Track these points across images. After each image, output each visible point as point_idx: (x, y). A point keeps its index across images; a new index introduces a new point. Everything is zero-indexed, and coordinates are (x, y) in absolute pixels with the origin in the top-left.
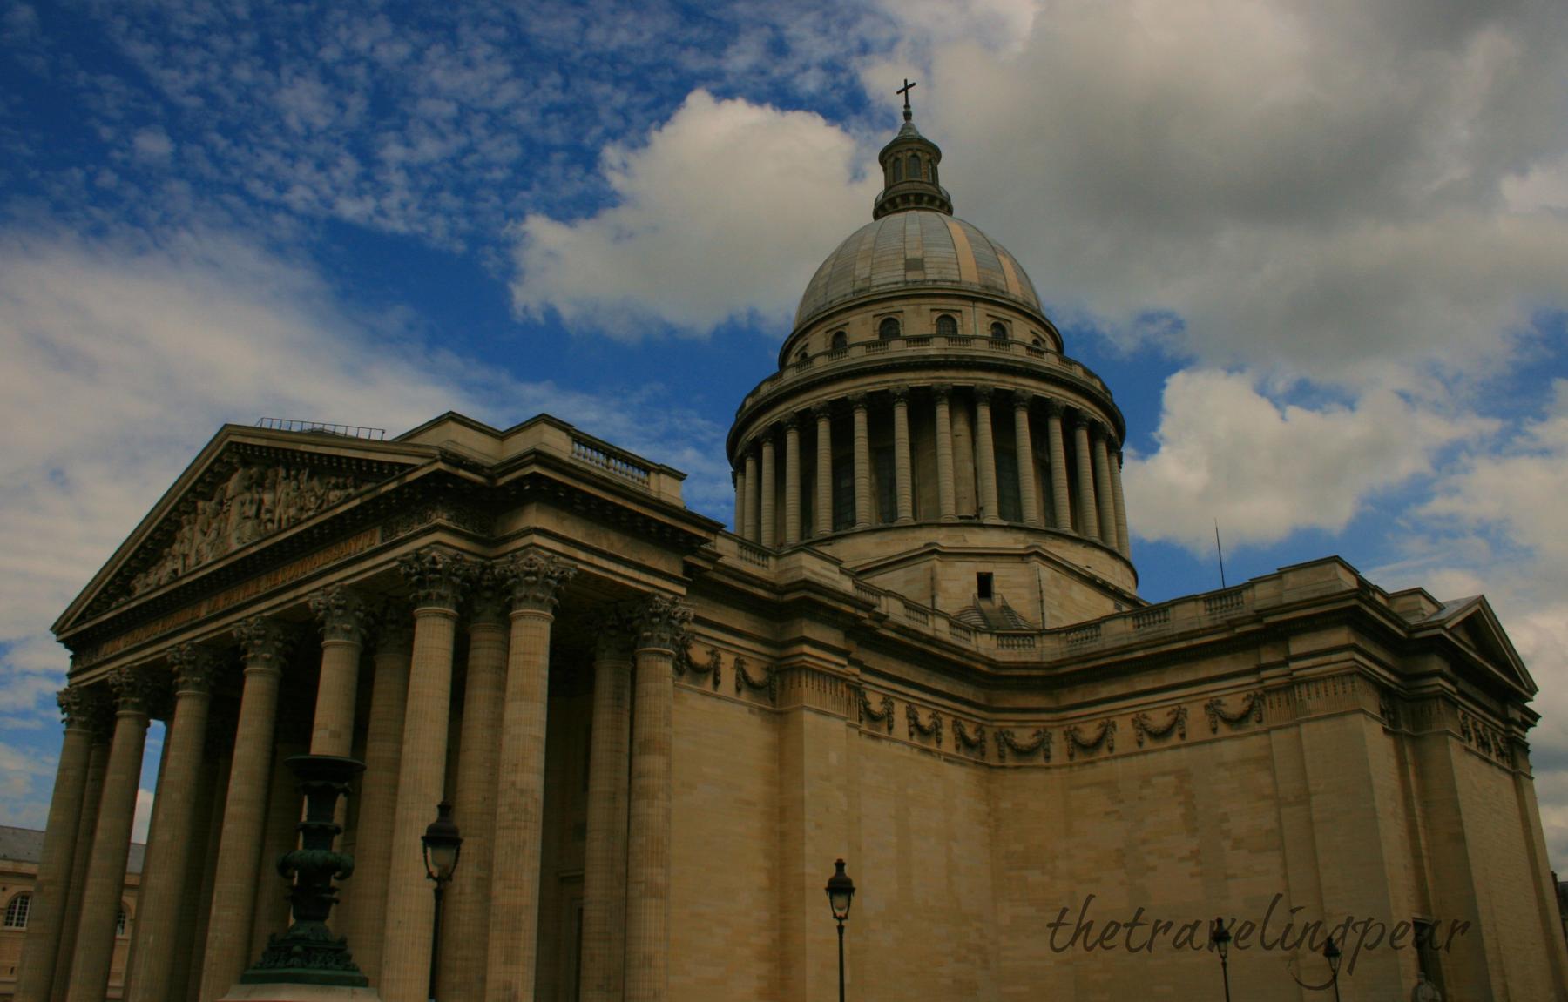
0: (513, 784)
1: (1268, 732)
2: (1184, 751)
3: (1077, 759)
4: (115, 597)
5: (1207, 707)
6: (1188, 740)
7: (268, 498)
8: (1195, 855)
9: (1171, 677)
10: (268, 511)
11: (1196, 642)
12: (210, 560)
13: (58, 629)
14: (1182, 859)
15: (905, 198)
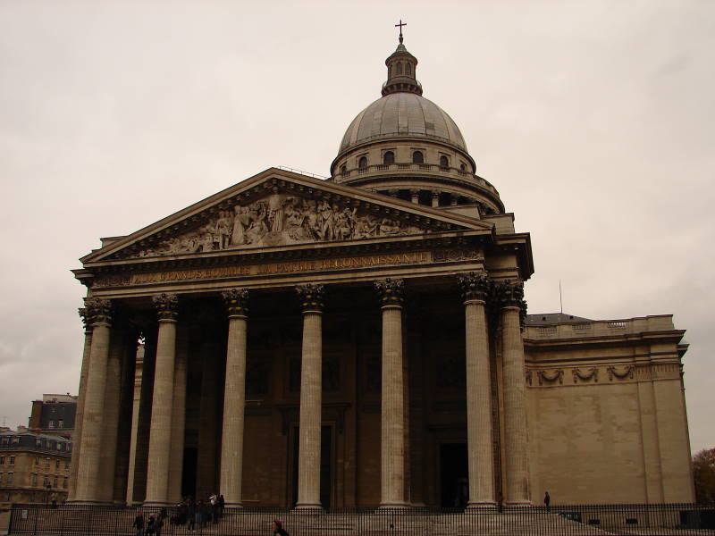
0: (518, 388)
1: (637, 383)
2: (597, 388)
3: (544, 386)
4: (145, 249)
5: (608, 369)
6: (599, 382)
7: (313, 217)
8: (600, 432)
9: (592, 355)
10: (317, 225)
11: (608, 341)
12: (260, 244)
13: (85, 260)
14: (594, 433)
15: (406, 85)
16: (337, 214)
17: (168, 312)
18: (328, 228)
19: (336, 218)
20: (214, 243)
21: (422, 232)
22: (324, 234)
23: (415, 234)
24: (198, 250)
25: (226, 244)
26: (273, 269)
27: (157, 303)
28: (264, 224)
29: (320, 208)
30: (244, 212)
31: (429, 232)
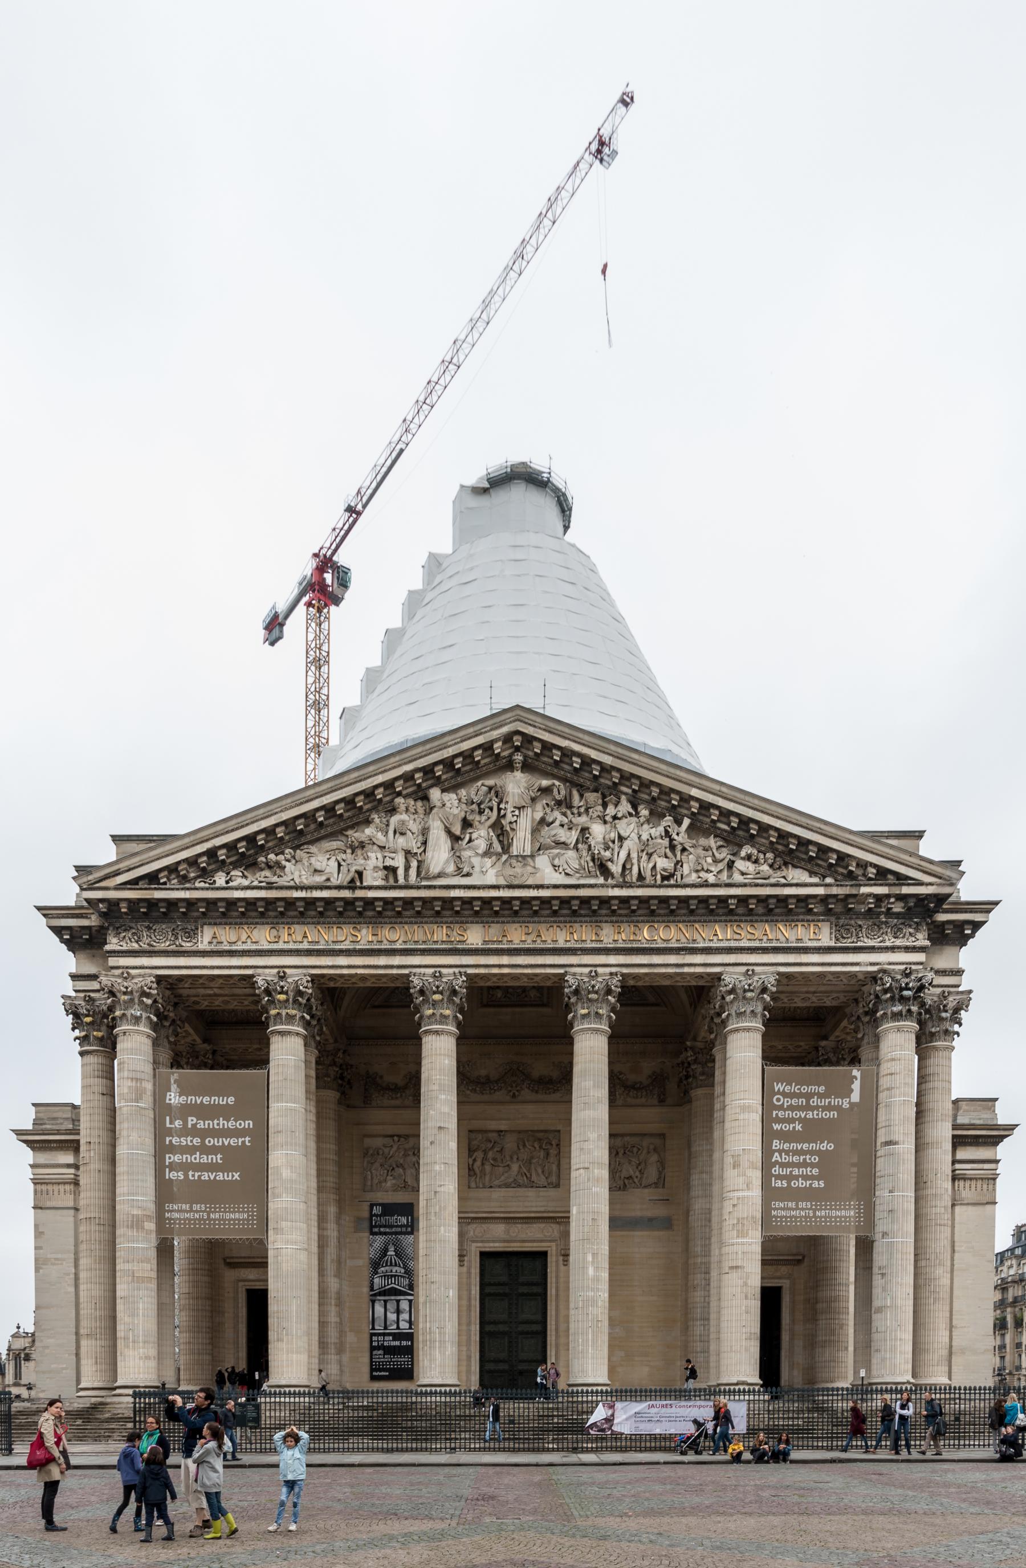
16: (646, 826)
17: (294, 1012)
18: (629, 854)
19: (645, 837)
20: (386, 868)
21: (815, 880)
22: (620, 870)
23: (799, 882)
24: (352, 881)
25: (413, 872)
26: (517, 935)
27: (268, 992)
28: (492, 834)
29: (611, 810)
30: (450, 804)
31: (829, 880)
